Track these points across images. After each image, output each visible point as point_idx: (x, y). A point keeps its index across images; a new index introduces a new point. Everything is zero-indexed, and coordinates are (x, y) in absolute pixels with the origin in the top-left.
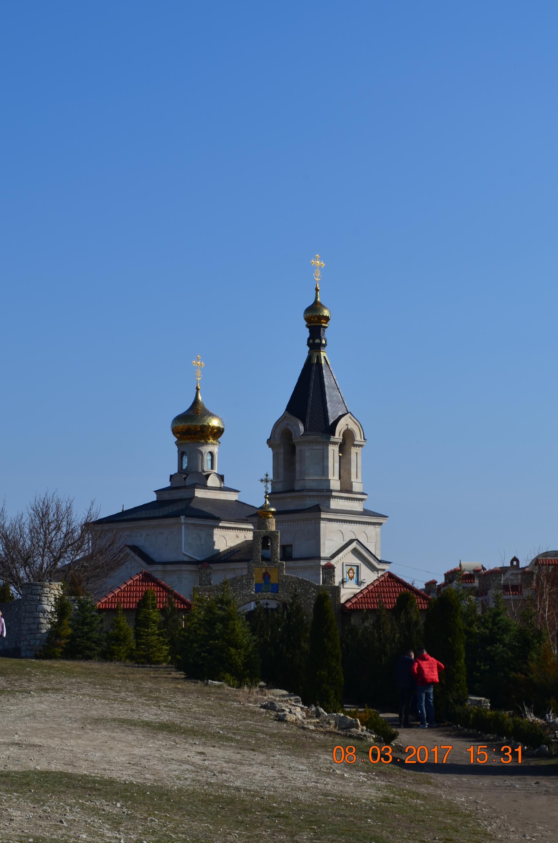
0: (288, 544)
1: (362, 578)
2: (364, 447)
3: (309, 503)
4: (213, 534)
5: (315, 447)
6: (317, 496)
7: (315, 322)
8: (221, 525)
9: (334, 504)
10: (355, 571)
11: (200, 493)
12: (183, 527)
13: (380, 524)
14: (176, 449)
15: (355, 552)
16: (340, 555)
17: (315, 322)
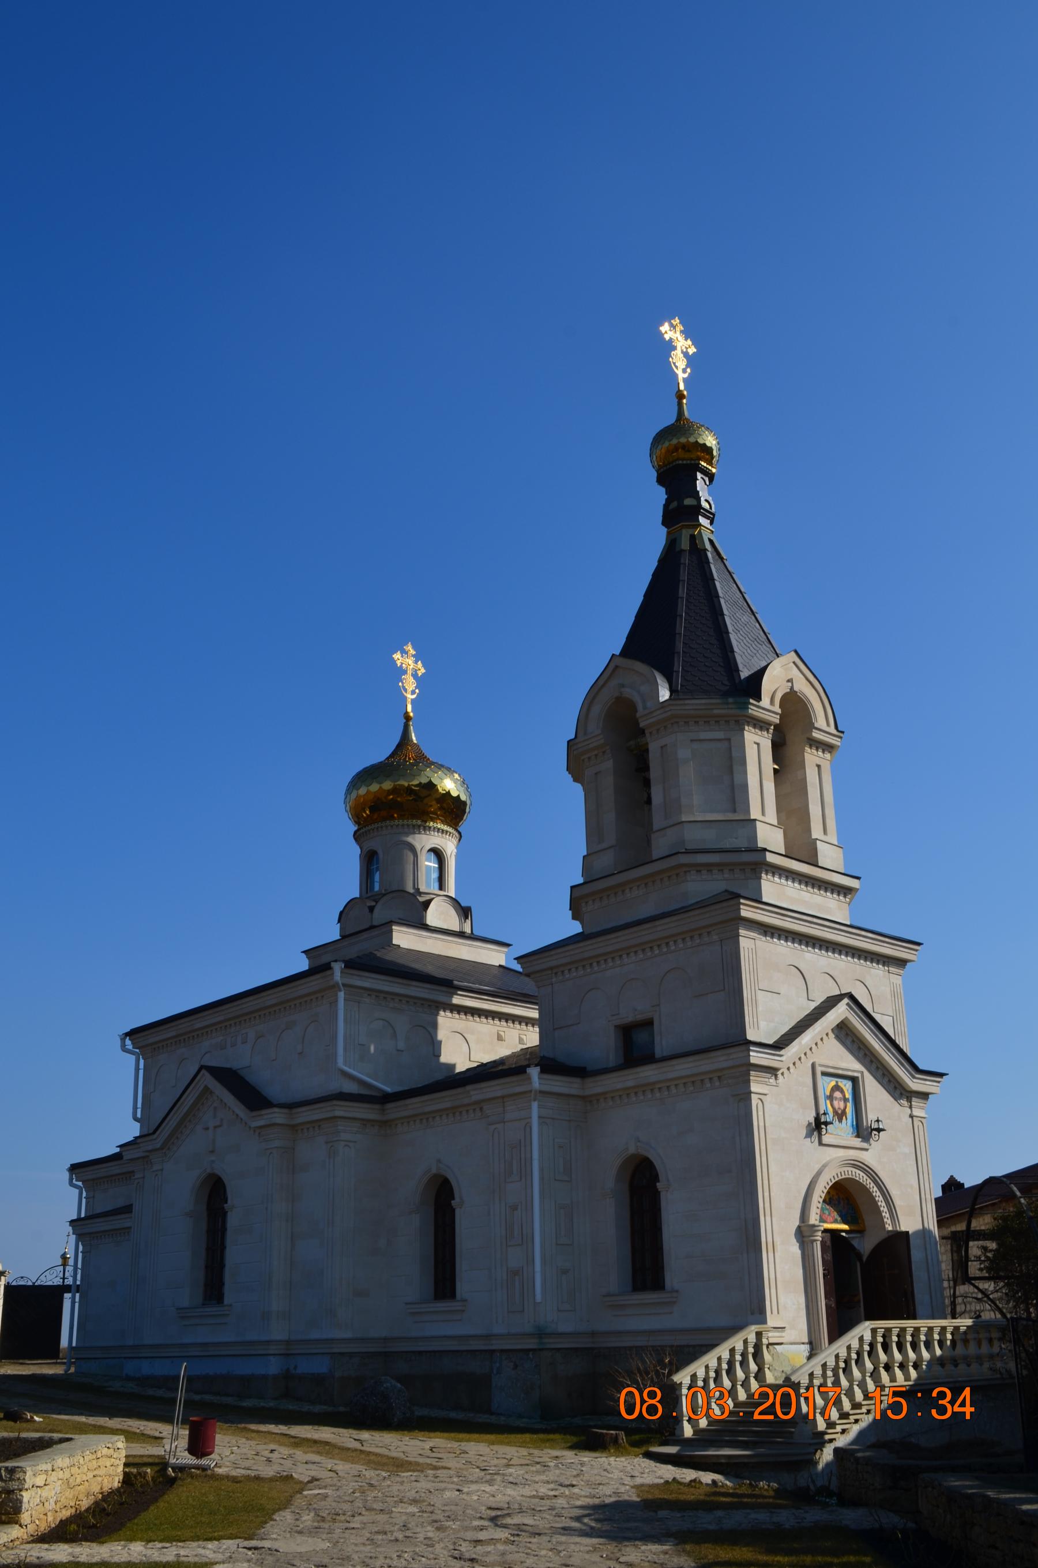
0: (640, 1017)
1: (871, 1116)
2: (837, 753)
3: (699, 887)
4: (435, 1025)
5: (703, 735)
6: (720, 866)
7: (679, 465)
8: (456, 1000)
9: (772, 888)
10: (849, 1095)
11: (404, 938)
12: (341, 995)
13: (901, 963)
14: (356, 850)
15: (844, 1032)
16: (807, 1038)
17: (679, 465)
